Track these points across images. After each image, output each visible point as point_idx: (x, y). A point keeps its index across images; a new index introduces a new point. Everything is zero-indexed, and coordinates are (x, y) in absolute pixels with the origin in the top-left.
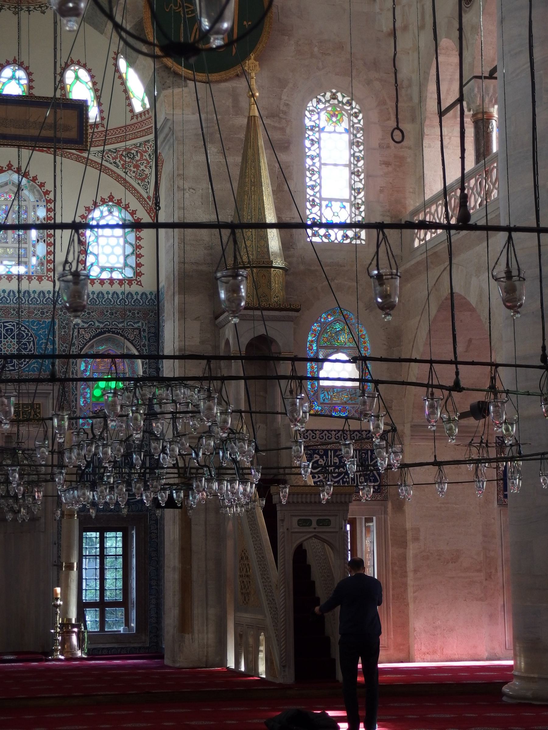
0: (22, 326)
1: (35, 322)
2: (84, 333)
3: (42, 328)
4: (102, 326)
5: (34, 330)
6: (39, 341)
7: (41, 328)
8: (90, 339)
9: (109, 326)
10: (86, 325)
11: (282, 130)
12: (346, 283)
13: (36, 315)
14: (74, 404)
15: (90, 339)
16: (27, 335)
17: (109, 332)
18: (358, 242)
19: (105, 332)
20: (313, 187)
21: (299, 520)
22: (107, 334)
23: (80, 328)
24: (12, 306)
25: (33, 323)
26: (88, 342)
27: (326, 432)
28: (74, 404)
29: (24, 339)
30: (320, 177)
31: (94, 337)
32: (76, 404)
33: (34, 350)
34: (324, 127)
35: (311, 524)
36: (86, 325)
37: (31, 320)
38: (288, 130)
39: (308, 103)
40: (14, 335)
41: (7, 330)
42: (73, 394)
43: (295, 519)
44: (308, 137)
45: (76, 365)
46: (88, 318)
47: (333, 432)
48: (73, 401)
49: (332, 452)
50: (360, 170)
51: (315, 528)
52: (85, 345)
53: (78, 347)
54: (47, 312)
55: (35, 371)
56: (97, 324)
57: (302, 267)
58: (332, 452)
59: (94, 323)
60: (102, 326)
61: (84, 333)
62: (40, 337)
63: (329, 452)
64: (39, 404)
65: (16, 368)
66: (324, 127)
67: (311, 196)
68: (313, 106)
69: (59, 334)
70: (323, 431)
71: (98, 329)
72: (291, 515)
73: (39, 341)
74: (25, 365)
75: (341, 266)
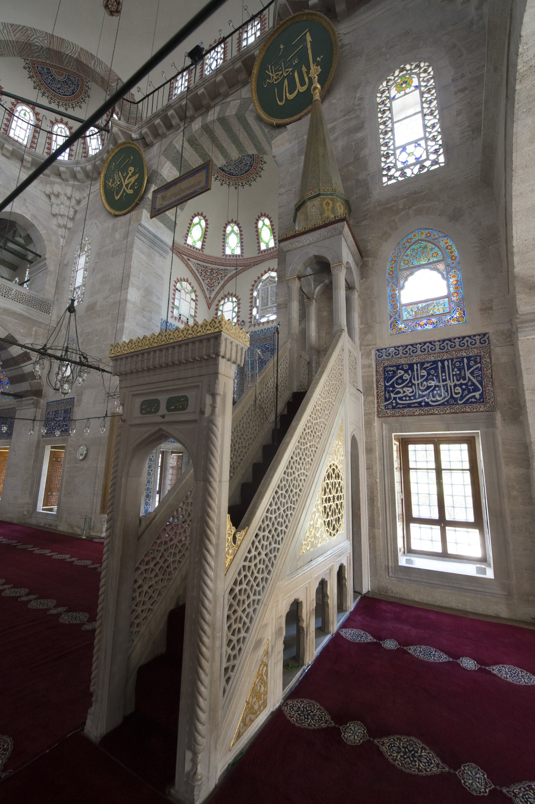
11: (358, 117)
12: (425, 205)
18: (437, 166)
20: (386, 144)
21: (143, 403)
27: (410, 347)
30: (393, 134)
34: (395, 96)
35: (157, 410)
38: (362, 115)
39: (379, 86)
43: (138, 401)
44: (380, 110)
47: (419, 346)
49: (419, 365)
50: (434, 109)
51: (163, 417)
57: (378, 209)
58: (419, 365)
63: (415, 365)
66: (395, 96)
67: (384, 151)
68: (383, 87)
70: (407, 346)
72: (133, 395)
75: (418, 193)
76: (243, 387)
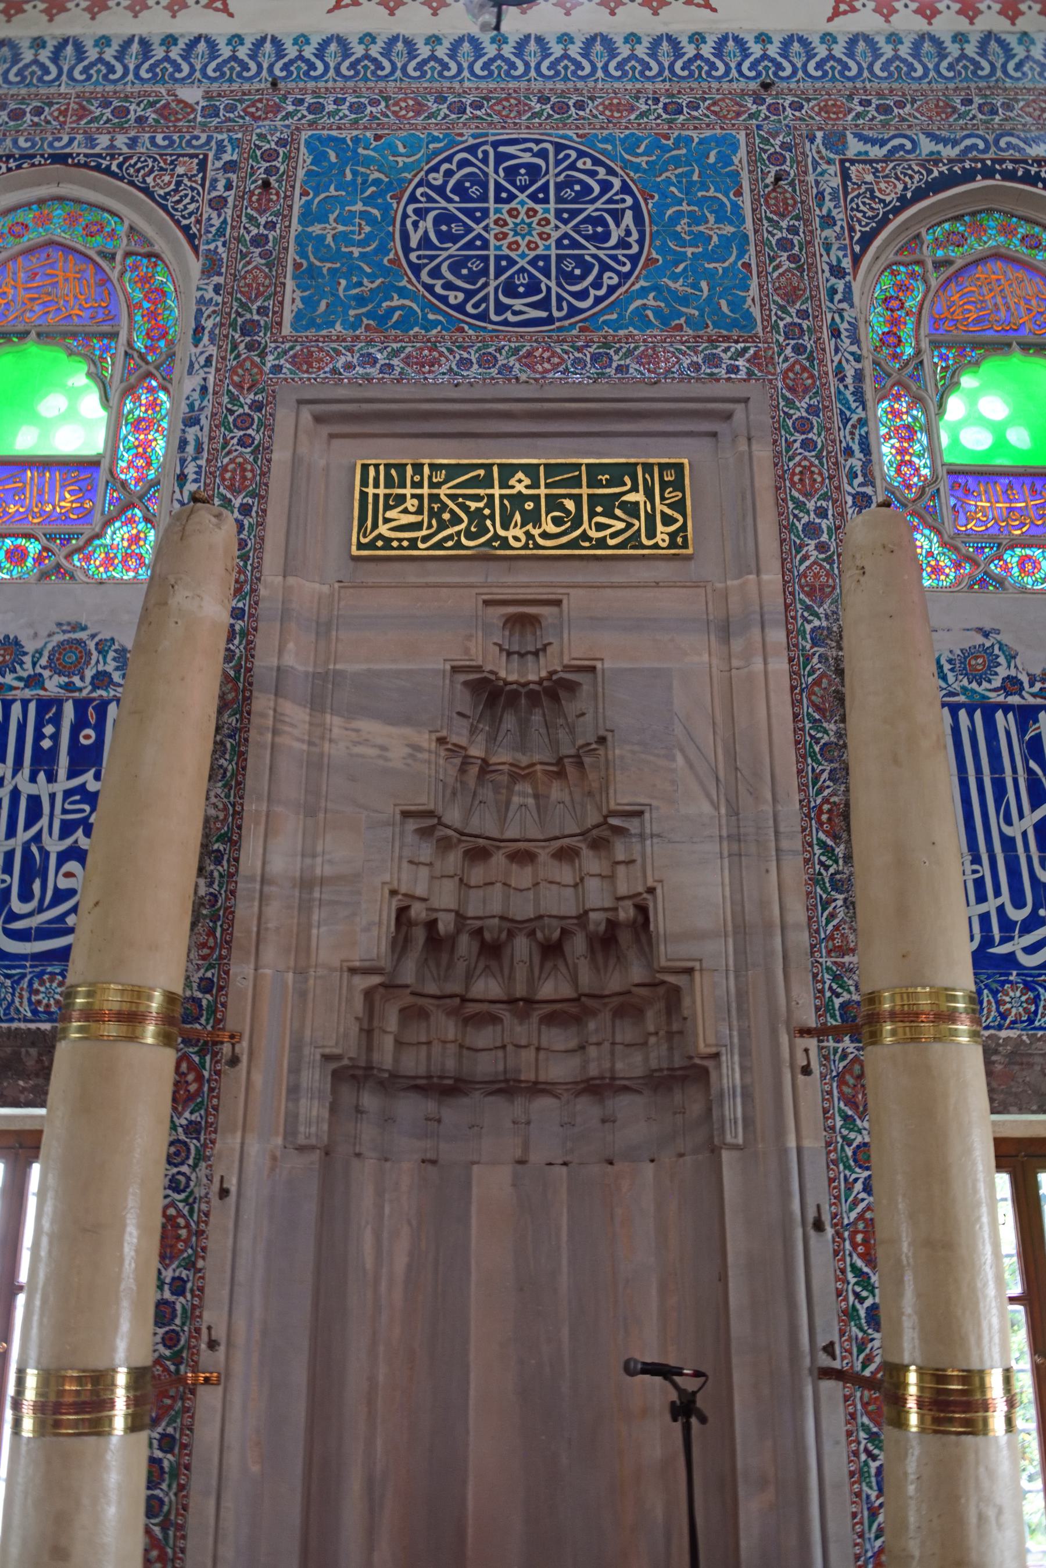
0: (581, 154)
1: (639, 141)
2: (869, 178)
3: (677, 161)
4: (949, 152)
5: (637, 168)
6: (661, 207)
7: (667, 162)
8: (902, 198)
9: (984, 152)
10: (876, 152)
13: (643, 115)
14: (856, 462)
15: (905, 203)
16: (606, 186)
17: (988, 173)
19: (968, 176)
22: (980, 183)
23: (853, 162)
24: (537, 85)
25: (631, 145)
26: (897, 211)
28: (856, 462)
29: (593, 201)
31: (920, 194)
32: (867, 464)
33: (641, 242)
36: (876, 152)
37: (619, 134)
40: (545, 188)
41: (511, 173)
42: (846, 420)
45: (848, 297)
46: (885, 124)
48: (849, 452)
52: (884, 222)
53: (852, 229)
54: (693, 106)
55: (649, 324)
56: (927, 146)
59: (913, 141)
60: (949, 152)
61: (869, 178)
62: (664, 195)
64: (679, 468)
65: (556, 314)
69: (754, 182)
71: (936, 163)
73: (661, 207)
74: (598, 300)
76: (263, 451)
